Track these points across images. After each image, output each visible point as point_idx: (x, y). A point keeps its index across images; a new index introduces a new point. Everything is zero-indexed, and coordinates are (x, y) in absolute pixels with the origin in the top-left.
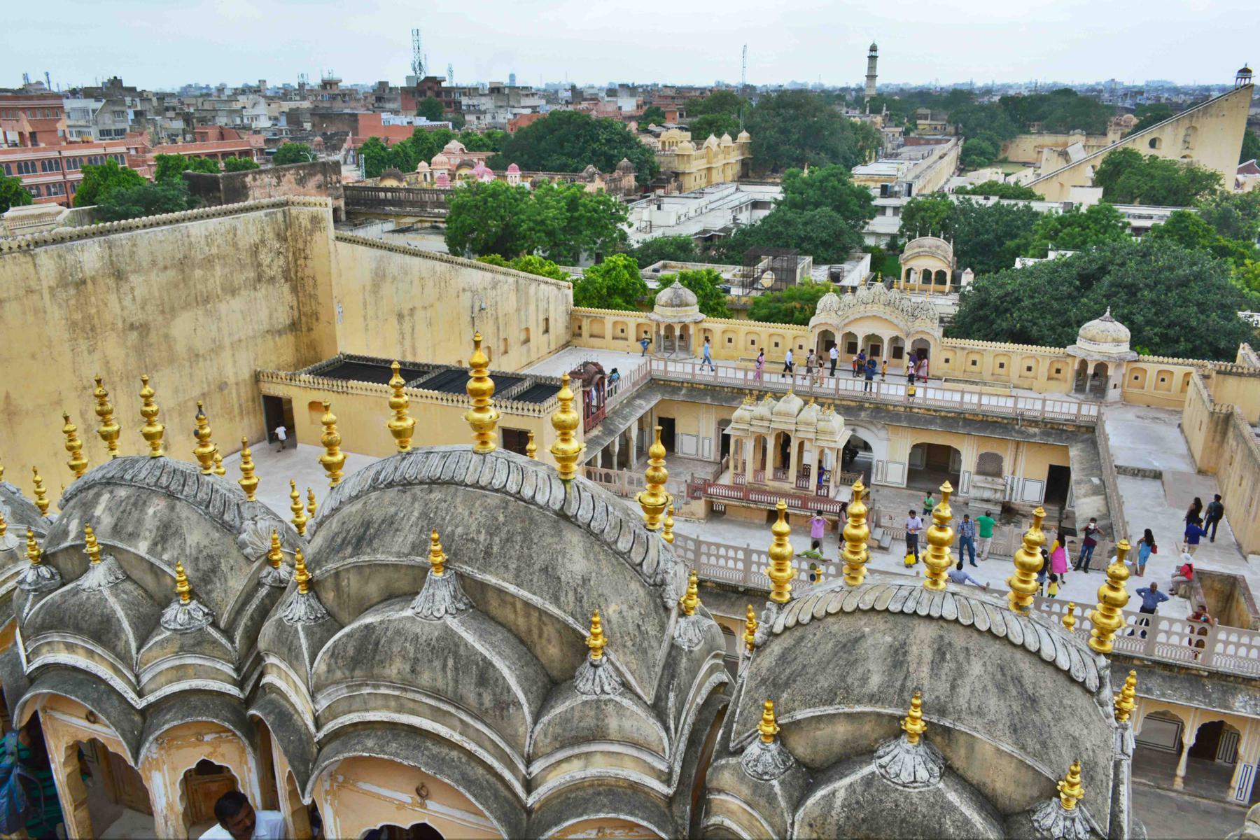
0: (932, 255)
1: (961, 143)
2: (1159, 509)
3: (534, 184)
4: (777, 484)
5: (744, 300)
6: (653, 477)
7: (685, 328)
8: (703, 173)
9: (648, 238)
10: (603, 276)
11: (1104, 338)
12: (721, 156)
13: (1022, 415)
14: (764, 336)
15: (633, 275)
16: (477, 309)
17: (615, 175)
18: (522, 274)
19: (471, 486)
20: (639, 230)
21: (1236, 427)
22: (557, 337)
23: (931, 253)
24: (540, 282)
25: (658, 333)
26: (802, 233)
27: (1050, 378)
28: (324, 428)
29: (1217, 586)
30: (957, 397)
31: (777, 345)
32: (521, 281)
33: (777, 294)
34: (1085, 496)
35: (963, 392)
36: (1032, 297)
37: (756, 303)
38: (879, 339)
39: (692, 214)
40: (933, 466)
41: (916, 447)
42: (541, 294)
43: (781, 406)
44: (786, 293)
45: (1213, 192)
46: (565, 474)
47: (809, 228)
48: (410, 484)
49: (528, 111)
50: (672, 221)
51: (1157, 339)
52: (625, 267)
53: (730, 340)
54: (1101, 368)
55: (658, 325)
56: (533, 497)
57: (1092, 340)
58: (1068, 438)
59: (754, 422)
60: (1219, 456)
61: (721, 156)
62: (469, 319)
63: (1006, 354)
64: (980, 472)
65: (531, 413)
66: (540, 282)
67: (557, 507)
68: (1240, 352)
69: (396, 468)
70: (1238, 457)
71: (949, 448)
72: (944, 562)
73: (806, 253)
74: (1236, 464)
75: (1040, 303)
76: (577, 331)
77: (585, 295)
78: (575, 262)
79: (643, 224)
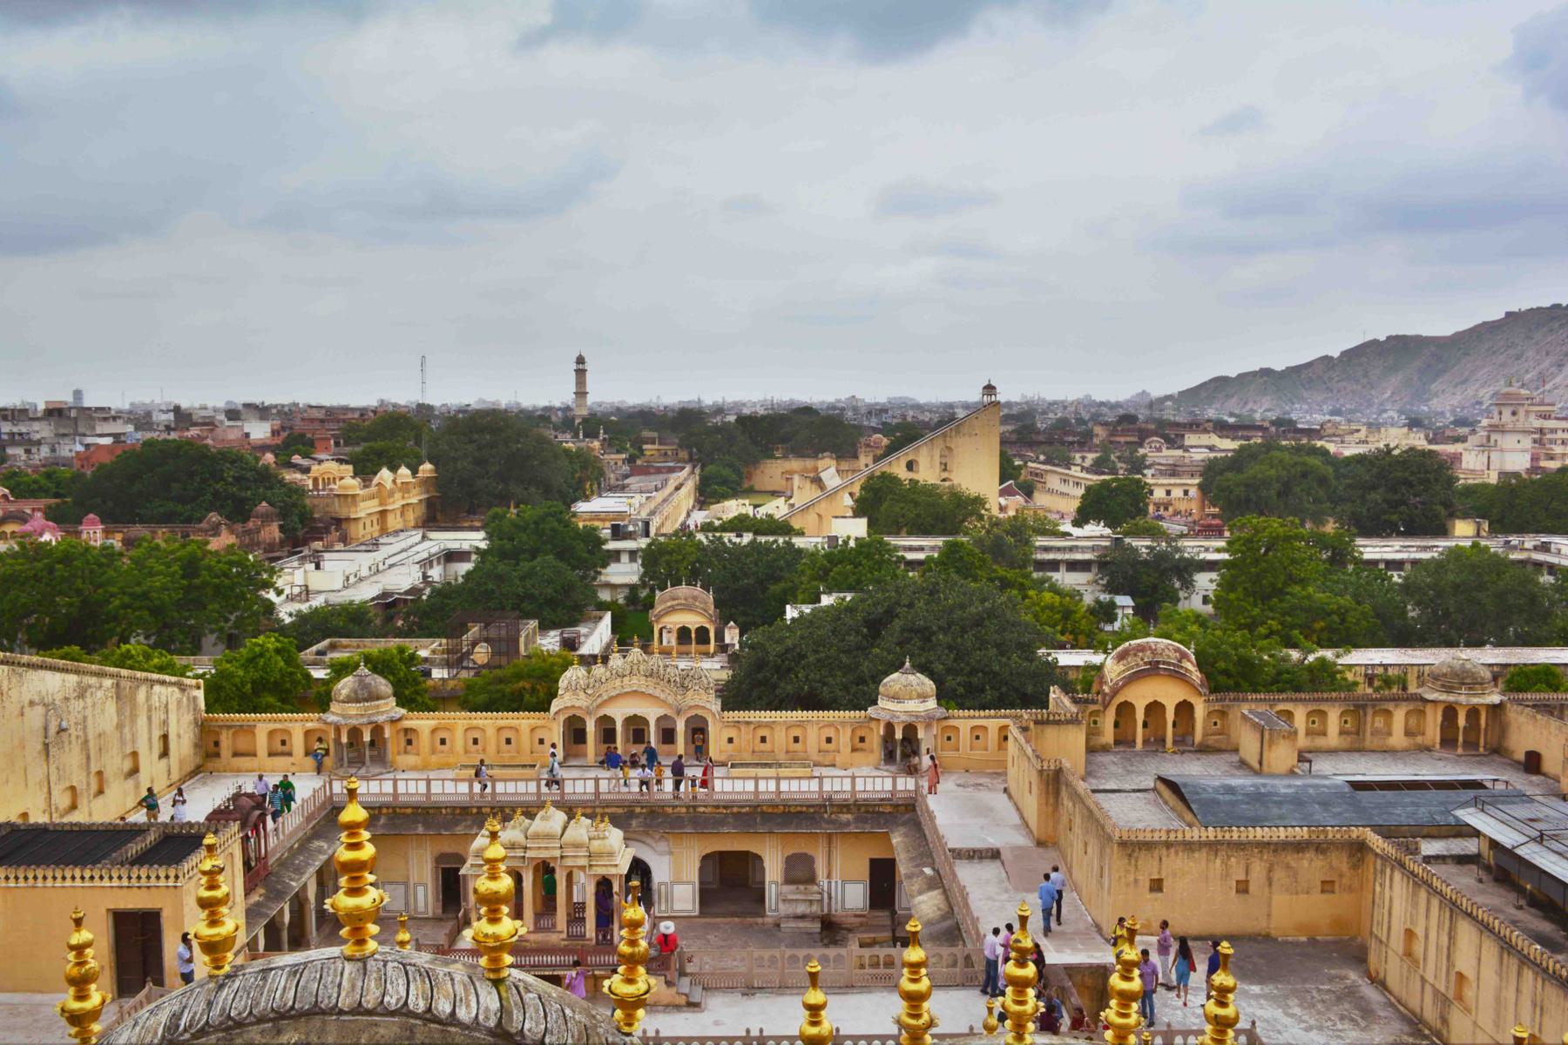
0: (688, 608)
1: (697, 471)
2: (1005, 896)
3: (128, 542)
4: (540, 937)
5: (451, 684)
6: (632, 955)
7: (377, 730)
9: (304, 607)
10: (245, 667)
11: (907, 695)
12: (398, 495)
13: (830, 799)
14: (491, 732)
15: (290, 661)
16: (53, 729)
17: (251, 524)
18: (124, 672)
19: (353, 1012)
20: (291, 599)
21: (1068, 785)
22: (181, 762)
24: (153, 683)
25: (337, 740)
26: (521, 591)
27: (854, 750)
28: (71, 956)
29: (1089, 981)
30: (750, 786)
31: (508, 741)
32: (123, 683)
33: (498, 672)
34: (920, 893)
35: (756, 779)
36: (816, 652)
37: (469, 687)
38: (645, 721)
39: (365, 572)
40: (730, 884)
41: (705, 858)
42: (155, 701)
43: (537, 825)
44: (508, 671)
45: (981, 517)
46: (497, 970)
47: (528, 583)
48: (239, 1024)
49: (107, 441)
50: (338, 585)
51: (961, 690)
52: (278, 651)
53: (443, 742)
54: (910, 729)
55: (338, 729)
56: (453, 1013)
57: (895, 698)
58: (887, 821)
60: (1057, 821)
61: (398, 495)
62: (40, 747)
63: (800, 724)
64: (789, 880)
65: (162, 883)
66: (153, 683)
67: (492, 1023)
68: (1052, 696)
69: (210, 1004)
70: (1078, 820)
71: (747, 853)
72: (1029, 1008)
73: (529, 616)
74: (1077, 830)
75: (827, 657)
76: (212, 748)
77: (220, 695)
78: (196, 649)
79: (296, 590)
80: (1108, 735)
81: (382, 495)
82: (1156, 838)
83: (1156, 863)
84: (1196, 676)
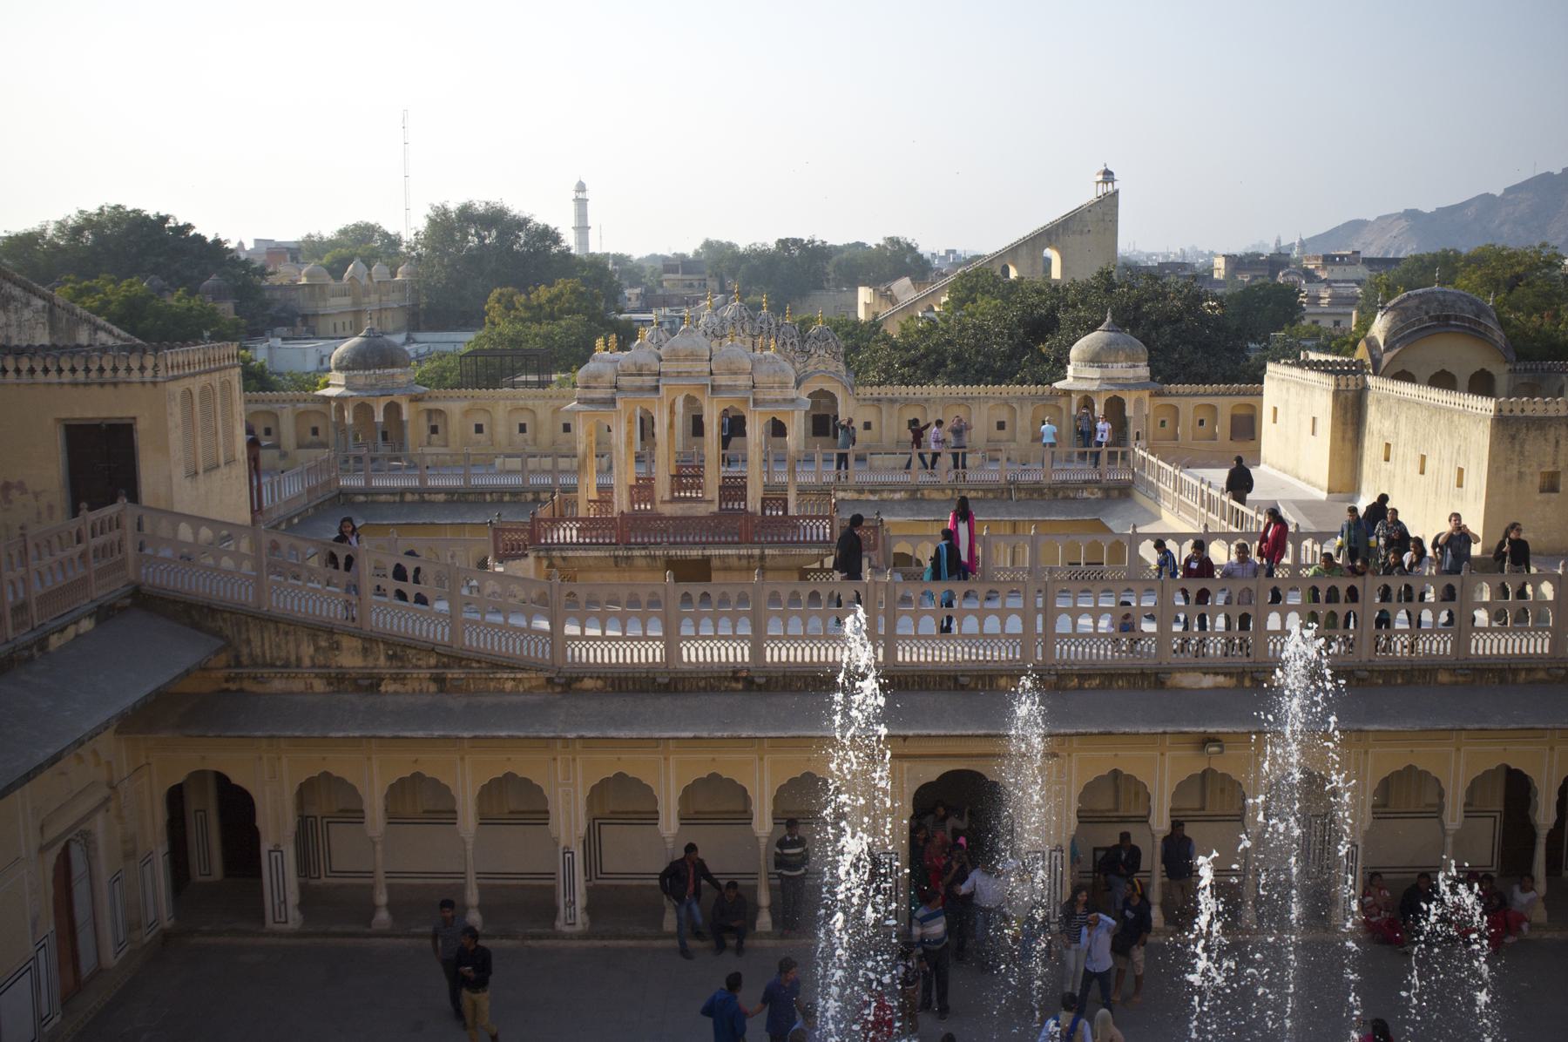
8: (348, 319)
32: (58, 311)
54: (1115, 408)
59: (624, 381)
63: (965, 401)
82: (1552, 413)
83: (1550, 449)
84: (1498, 335)
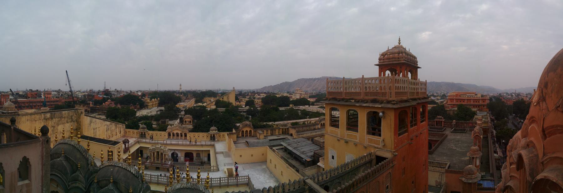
23: (188, 118)
54: (214, 135)
80: (241, 135)
81: (153, 102)
